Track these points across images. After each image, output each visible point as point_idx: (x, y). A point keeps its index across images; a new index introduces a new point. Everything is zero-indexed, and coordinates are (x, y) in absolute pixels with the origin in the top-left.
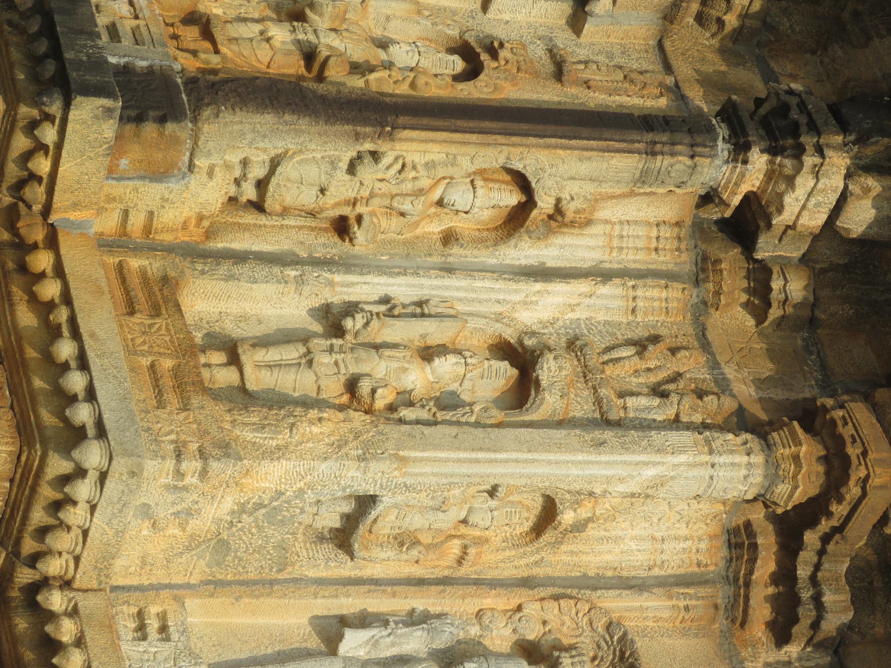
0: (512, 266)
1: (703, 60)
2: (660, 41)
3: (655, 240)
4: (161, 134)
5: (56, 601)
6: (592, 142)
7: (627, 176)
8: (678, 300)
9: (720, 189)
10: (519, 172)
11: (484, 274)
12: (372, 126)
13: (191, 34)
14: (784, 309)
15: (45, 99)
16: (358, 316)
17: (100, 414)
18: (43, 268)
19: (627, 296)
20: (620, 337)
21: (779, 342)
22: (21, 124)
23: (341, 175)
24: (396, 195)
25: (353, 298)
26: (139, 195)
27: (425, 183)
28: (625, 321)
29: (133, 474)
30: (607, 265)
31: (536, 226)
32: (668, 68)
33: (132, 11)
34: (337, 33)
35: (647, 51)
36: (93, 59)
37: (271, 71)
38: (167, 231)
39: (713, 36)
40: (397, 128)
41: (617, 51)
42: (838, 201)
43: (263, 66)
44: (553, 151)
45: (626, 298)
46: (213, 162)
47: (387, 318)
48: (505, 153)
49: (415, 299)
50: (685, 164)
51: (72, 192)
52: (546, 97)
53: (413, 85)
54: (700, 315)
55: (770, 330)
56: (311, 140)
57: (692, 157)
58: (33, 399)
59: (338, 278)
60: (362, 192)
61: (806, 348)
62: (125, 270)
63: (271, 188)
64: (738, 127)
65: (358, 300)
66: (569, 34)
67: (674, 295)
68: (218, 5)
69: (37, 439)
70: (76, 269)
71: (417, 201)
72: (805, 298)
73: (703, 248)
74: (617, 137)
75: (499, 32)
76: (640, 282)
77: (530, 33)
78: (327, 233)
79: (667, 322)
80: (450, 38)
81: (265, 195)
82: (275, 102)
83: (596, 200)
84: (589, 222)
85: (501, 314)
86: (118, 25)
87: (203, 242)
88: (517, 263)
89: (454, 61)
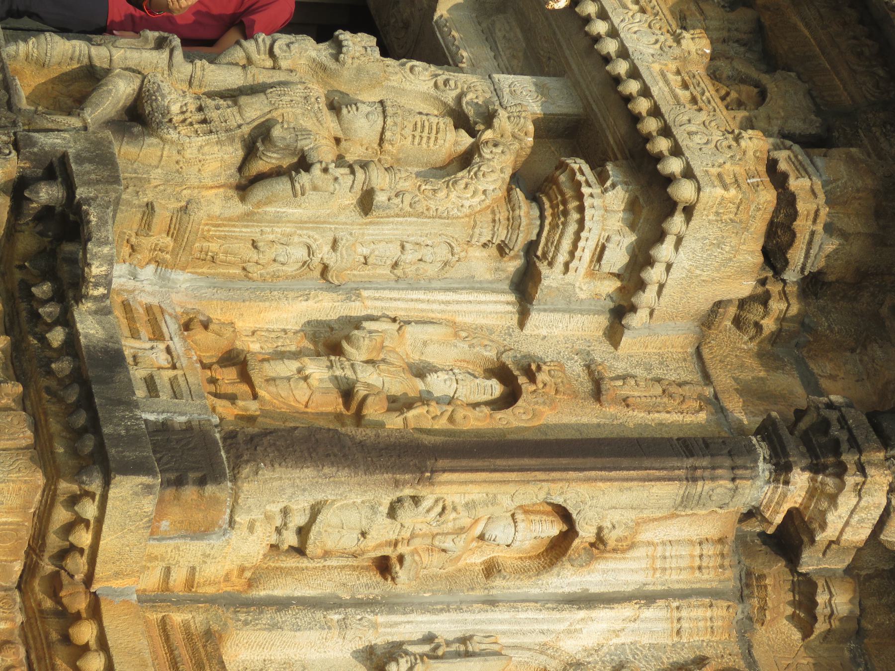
0: (556, 594)
1: (742, 366)
2: (698, 348)
3: (698, 559)
4: (201, 496)
6: (632, 472)
7: (668, 502)
8: (723, 618)
9: (762, 508)
10: (560, 505)
11: (528, 604)
12: (412, 472)
13: (228, 376)
14: (830, 622)
15: (84, 478)
16: (402, 661)
18: (86, 641)
19: (671, 617)
20: (665, 660)
21: (825, 655)
22: (61, 498)
23: (382, 519)
24: (437, 534)
25: (397, 638)
26: (181, 553)
27: (465, 521)
28: (670, 643)
30: (651, 588)
31: (578, 554)
32: (707, 377)
33: (170, 359)
34: (374, 366)
35: (685, 360)
36: (132, 432)
37: (309, 410)
38: (209, 584)
39: (751, 339)
40: (436, 471)
41: (655, 361)
42: (882, 517)
43: (301, 406)
44: (594, 484)
45: (670, 619)
46: (253, 517)
47: (432, 661)
48: (546, 490)
49: (459, 635)
50: (726, 488)
51: (113, 563)
52: (585, 420)
53: (451, 419)
54: (745, 632)
55: (817, 643)
56: (351, 490)
57: (733, 480)
59: (381, 619)
60: (402, 533)
61: (853, 660)
62: (168, 627)
63: (312, 536)
64: (778, 447)
65: (402, 639)
66: (607, 347)
67: (719, 614)
68: (255, 339)
70: (120, 642)
71: (459, 539)
72: (851, 612)
73: (747, 564)
74: (657, 465)
75: (537, 350)
76: (684, 603)
77: (567, 348)
78: (369, 572)
79: (713, 641)
80: (487, 359)
81: (306, 542)
82: (314, 455)
83: (638, 524)
84: (632, 546)
85: (545, 644)
86: (156, 378)
87: (245, 591)
88: (560, 591)
89: (491, 386)
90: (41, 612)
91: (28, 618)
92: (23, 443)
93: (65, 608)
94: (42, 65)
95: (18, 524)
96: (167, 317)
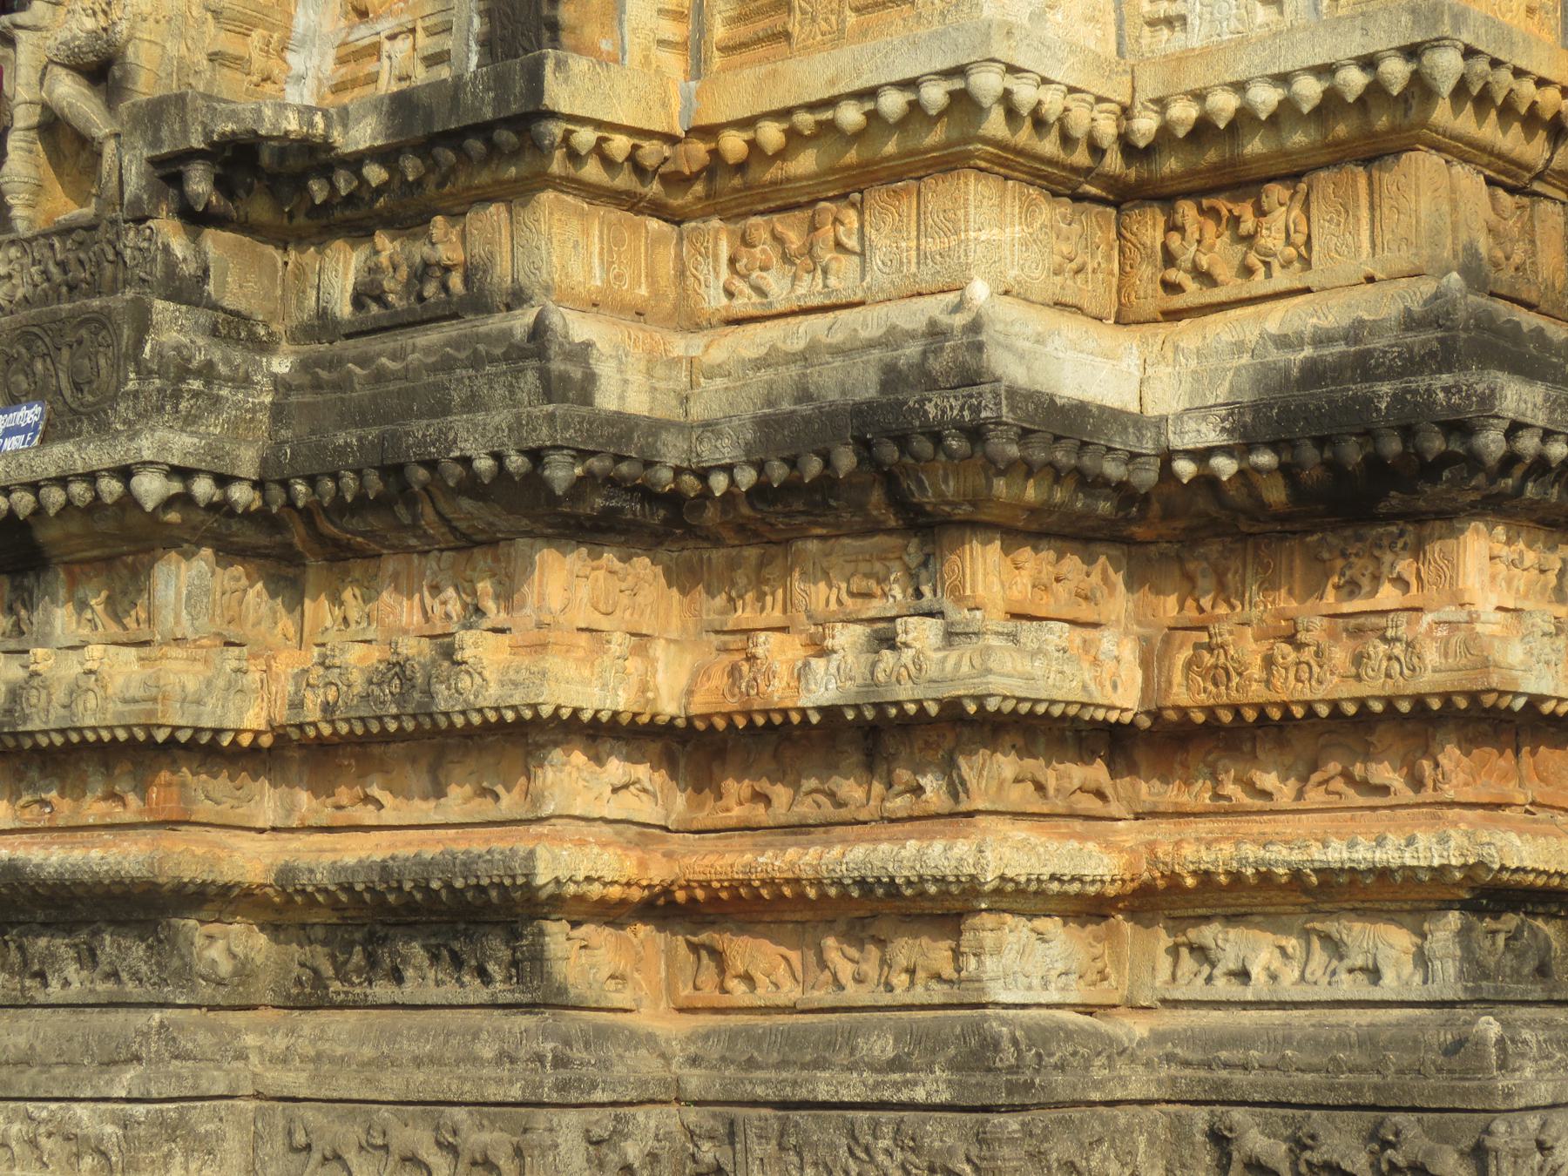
5: (1145, 125)
17: (936, 73)
22: (571, 170)
29: (1009, 33)
58: (911, 153)
69: (963, 148)
90: (708, 197)
91: (715, 212)
92: (504, 215)
93: (706, 168)
94: (39, 188)
95: (602, 223)
96: (351, 38)
